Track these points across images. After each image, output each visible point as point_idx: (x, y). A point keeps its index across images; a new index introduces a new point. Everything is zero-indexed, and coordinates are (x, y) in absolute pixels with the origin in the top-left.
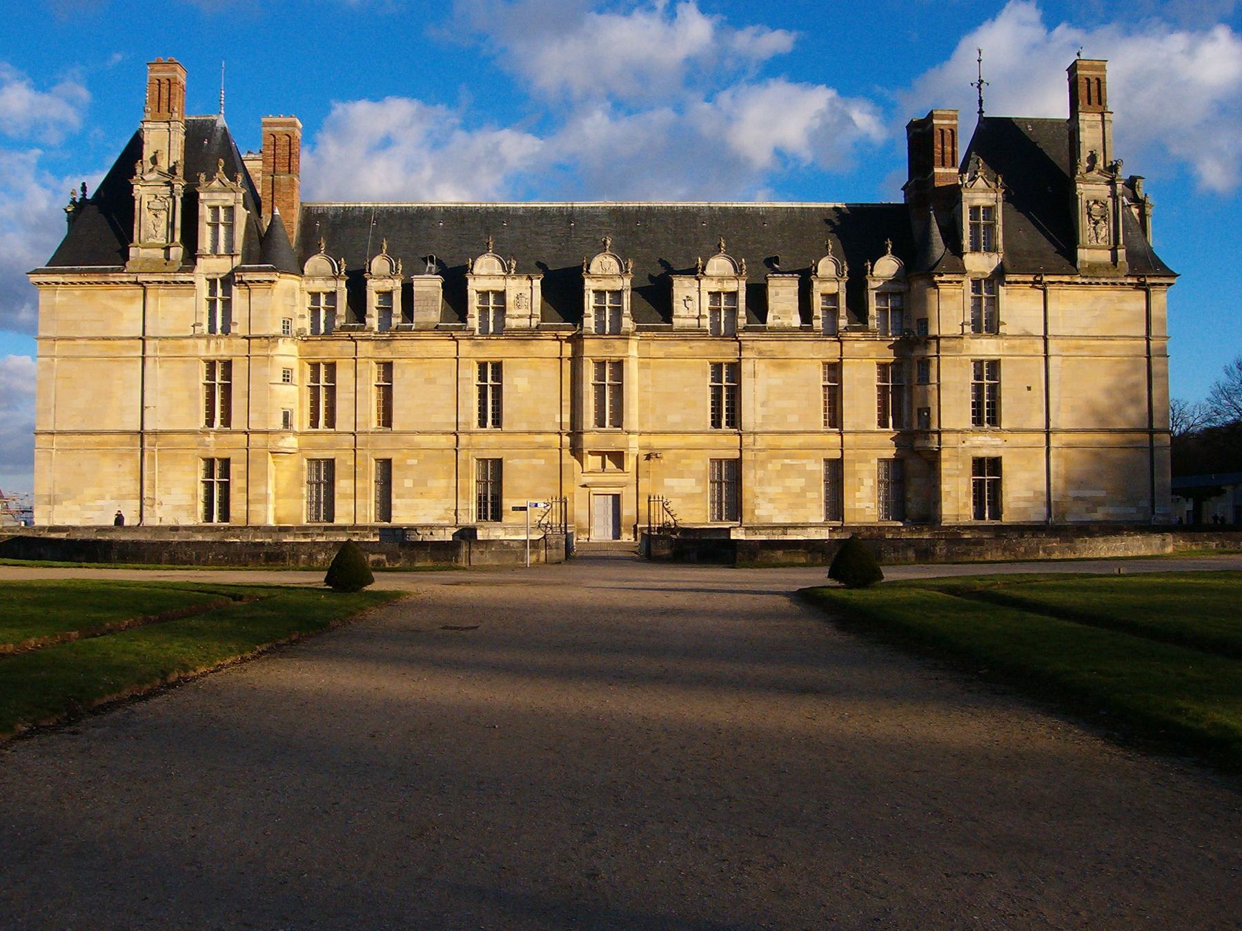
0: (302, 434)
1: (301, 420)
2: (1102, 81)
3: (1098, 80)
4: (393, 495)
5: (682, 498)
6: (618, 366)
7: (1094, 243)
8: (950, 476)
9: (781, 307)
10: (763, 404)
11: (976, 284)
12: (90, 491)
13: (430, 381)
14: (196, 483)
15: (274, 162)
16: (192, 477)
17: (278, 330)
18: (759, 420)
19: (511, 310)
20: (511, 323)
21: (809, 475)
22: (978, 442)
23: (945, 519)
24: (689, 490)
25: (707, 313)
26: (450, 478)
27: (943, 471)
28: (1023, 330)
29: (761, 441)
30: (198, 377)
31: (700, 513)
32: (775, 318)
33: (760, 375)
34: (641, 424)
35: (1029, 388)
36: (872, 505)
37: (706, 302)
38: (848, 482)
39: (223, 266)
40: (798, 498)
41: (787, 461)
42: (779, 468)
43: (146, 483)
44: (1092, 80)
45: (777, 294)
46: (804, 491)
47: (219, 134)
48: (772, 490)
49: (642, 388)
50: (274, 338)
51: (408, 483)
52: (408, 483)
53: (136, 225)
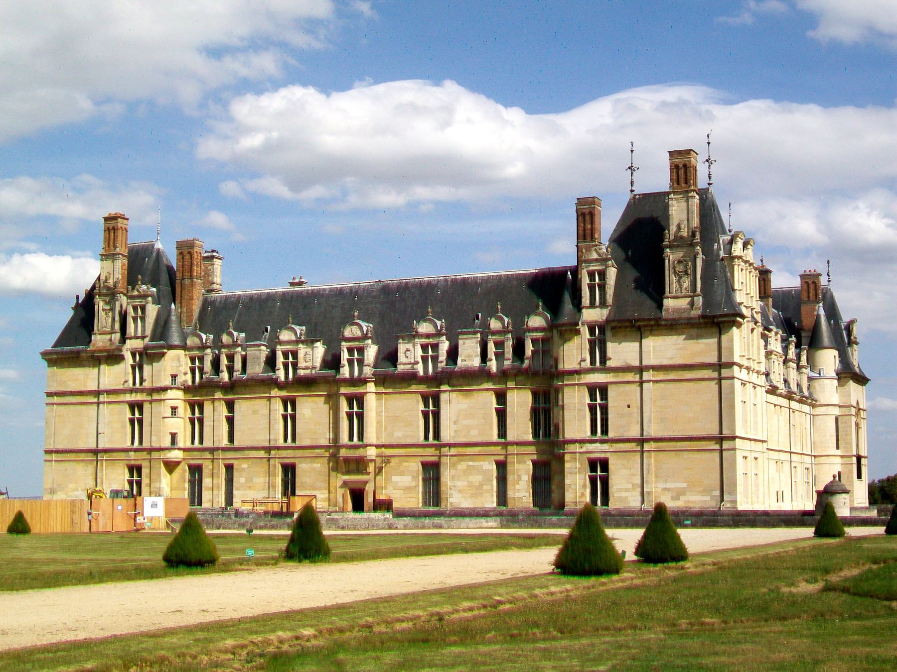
0: (185, 450)
1: (184, 440)
2: (688, 166)
3: (685, 166)
4: (234, 488)
5: (403, 490)
6: (360, 399)
7: (679, 294)
8: (571, 473)
9: (469, 351)
10: (455, 423)
11: (592, 331)
12: (71, 486)
13: (255, 412)
14: (124, 480)
15: (183, 270)
16: (122, 477)
17: (167, 382)
18: (453, 434)
19: (302, 364)
20: (301, 372)
21: (485, 473)
22: (591, 448)
23: (567, 505)
24: (407, 484)
25: (420, 360)
26: (266, 477)
27: (566, 470)
28: (625, 362)
29: (453, 451)
30: (126, 414)
31: (414, 500)
32: (463, 360)
33: (453, 402)
34: (378, 438)
35: (629, 406)
36: (527, 494)
37: (419, 352)
38: (510, 478)
39: (138, 344)
40: (478, 490)
41: (471, 463)
42: (465, 467)
43: (99, 481)
44: (681, 166)
45: (464, 343)
46: (481, 485)
47: (154, 254)
48: (460, 484)
49: (378, 414)
50: (165, 389)
51: (243, 480)
52: (243, 480)
53: (96, 321)
